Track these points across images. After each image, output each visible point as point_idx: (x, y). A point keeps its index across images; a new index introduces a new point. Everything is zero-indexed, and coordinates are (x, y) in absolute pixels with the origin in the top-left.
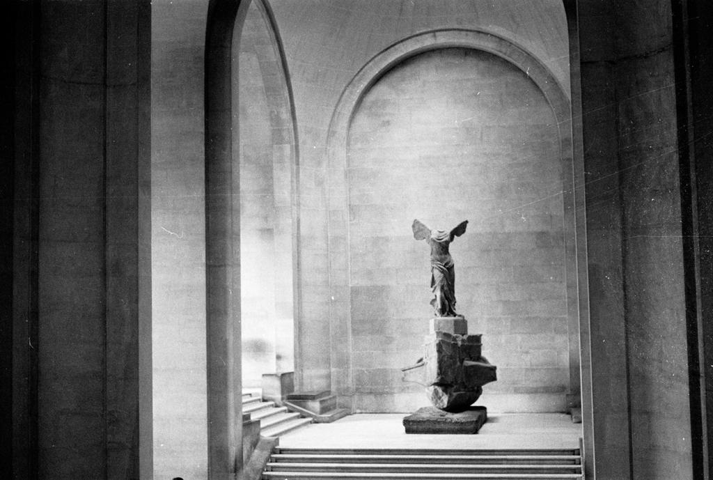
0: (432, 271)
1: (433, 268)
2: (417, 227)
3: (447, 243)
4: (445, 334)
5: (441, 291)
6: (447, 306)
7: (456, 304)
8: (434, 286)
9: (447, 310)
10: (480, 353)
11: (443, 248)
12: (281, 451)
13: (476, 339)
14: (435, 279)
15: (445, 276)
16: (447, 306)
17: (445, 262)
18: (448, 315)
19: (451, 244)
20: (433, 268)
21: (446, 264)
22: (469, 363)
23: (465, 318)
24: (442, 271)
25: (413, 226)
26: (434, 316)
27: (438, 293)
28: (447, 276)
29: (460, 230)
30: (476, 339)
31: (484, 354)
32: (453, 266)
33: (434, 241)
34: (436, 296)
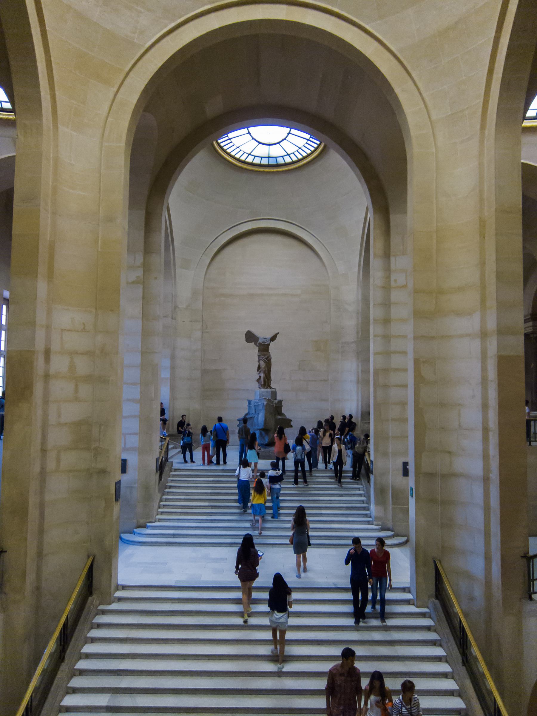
0: (259, 361)
3: (269, 345)
4: (269, 400)
11: (264, 349)
12: (176, 470)
13: (280, 402)
15: (266, 365)
18: (267, 388)
21: (268, 357)
22: (279, 417)
24: (265, 362)
25: (246, 335)
27: (262, 375)
29: (273, 338)
30: (280, 402)
34: (260, 377)
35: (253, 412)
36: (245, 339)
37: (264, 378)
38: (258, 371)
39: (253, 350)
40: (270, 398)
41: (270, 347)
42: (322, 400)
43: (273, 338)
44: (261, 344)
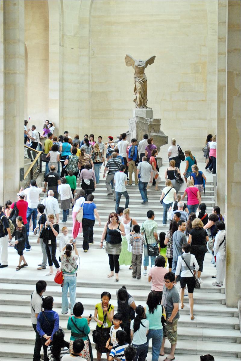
0: (135, 83)
1: (136, 81)
3: (143, 68)
4: (141, 118)
5: (140, 94)
6: (143, 102)
11: (140, 71)
13: (158, 121)
14: (137, 88)
15: (142, 86)
16: (143, 102)
18: (143, 107)
19: (145, 69)
21: (143, 79)
23: (152, 109)
24: (141, 83)
25: (126, 59)
26: (136, 108)
27: (138, 95)
28: (143, 85)
29: (151, 61)
30: (158, 121)
31: (162, 129)
34: (137, 97)
37: (140, 99)
38: (134, 92)
42: (200, 119)
43: (151, 61)
44: (137, 67)
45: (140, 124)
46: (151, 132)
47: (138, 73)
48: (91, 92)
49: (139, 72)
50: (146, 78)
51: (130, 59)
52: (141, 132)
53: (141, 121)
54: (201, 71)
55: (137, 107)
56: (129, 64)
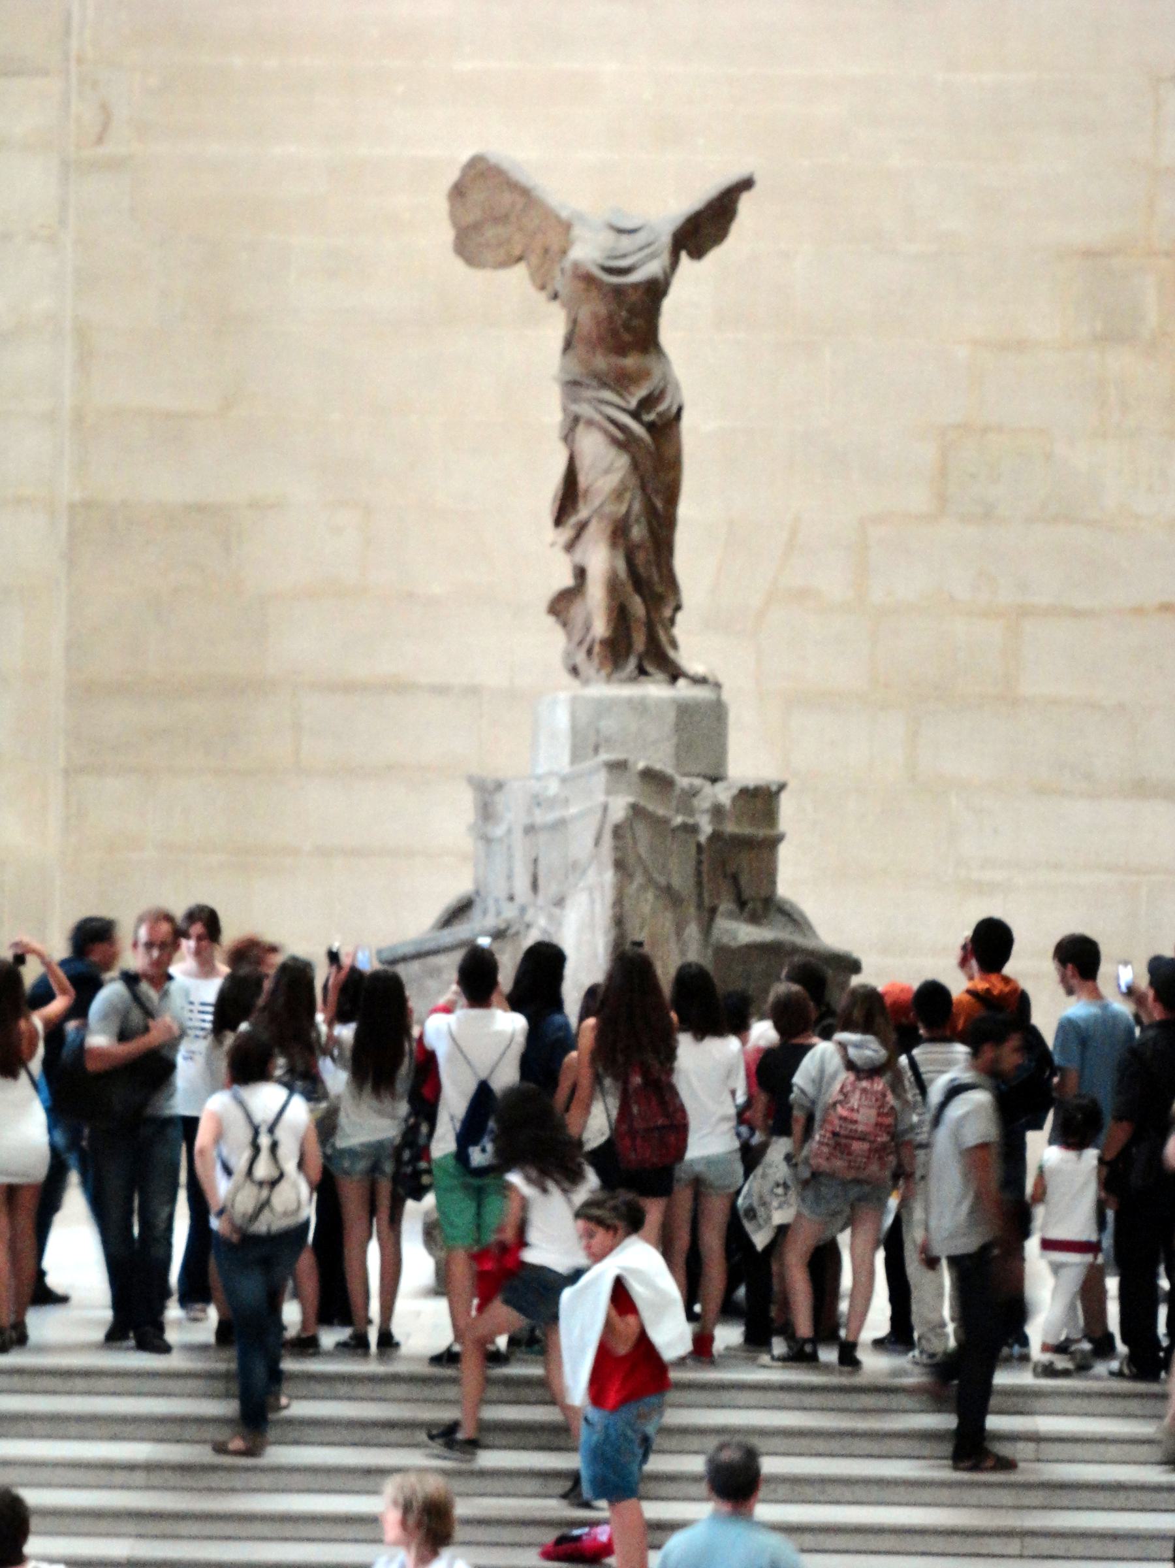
1: (576, 420)
2: (477, 196)
3: (656, 290)
4: (650, 776)
6: (637, 625)
7: (680, 617)
8: (573, 520)
9: (639, 641)
10: (773, 883)
11: (622, 324)
13: (761, 801)
14: (583, 480)
15: (635, 465)
16: (637, 625)
17: (642, 392)
18: (642, 671)
20: (576, 420)
21: (648, 402)
22: (746, 933)
23: (726, 696)
25: (458, 192)
26: (566, 678)
27: (599, 559)
28: (647, 464)
29: (704, 229)
30: (761, 801)
31: (785, 889)
32: (680, 409)
33: (588, 280)
34: (581, 573)
35: (521, 885)
36: (447, 234)
37: (613, 586)
39: (527, 340)
40: (663, 762)
41: (668, 305)
42: (1141, 788)
43: (704, 229)
45: (642, 832)
46: (713, 911)
47: (601, 339)
48: (72, 506)
49: (614, 333)
50: (677, 387)
51: (507, 198)
52: (646, 909)
53: (650, 807)
54: (1153, 318)
55: (589, 669)
56: (500, 245)
